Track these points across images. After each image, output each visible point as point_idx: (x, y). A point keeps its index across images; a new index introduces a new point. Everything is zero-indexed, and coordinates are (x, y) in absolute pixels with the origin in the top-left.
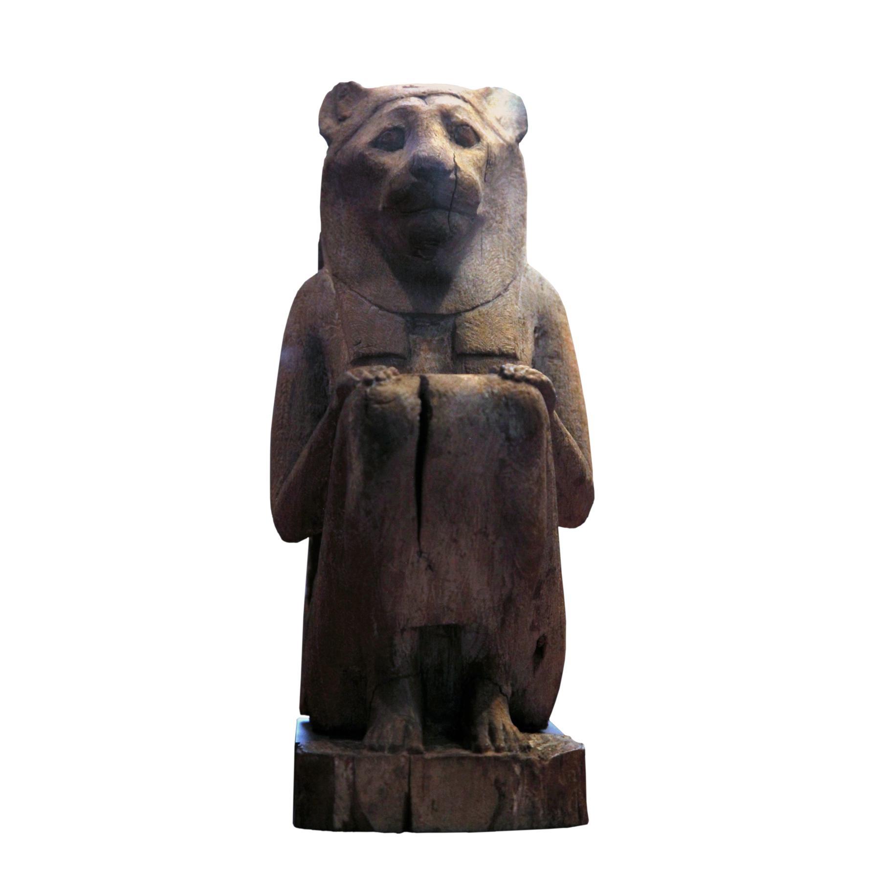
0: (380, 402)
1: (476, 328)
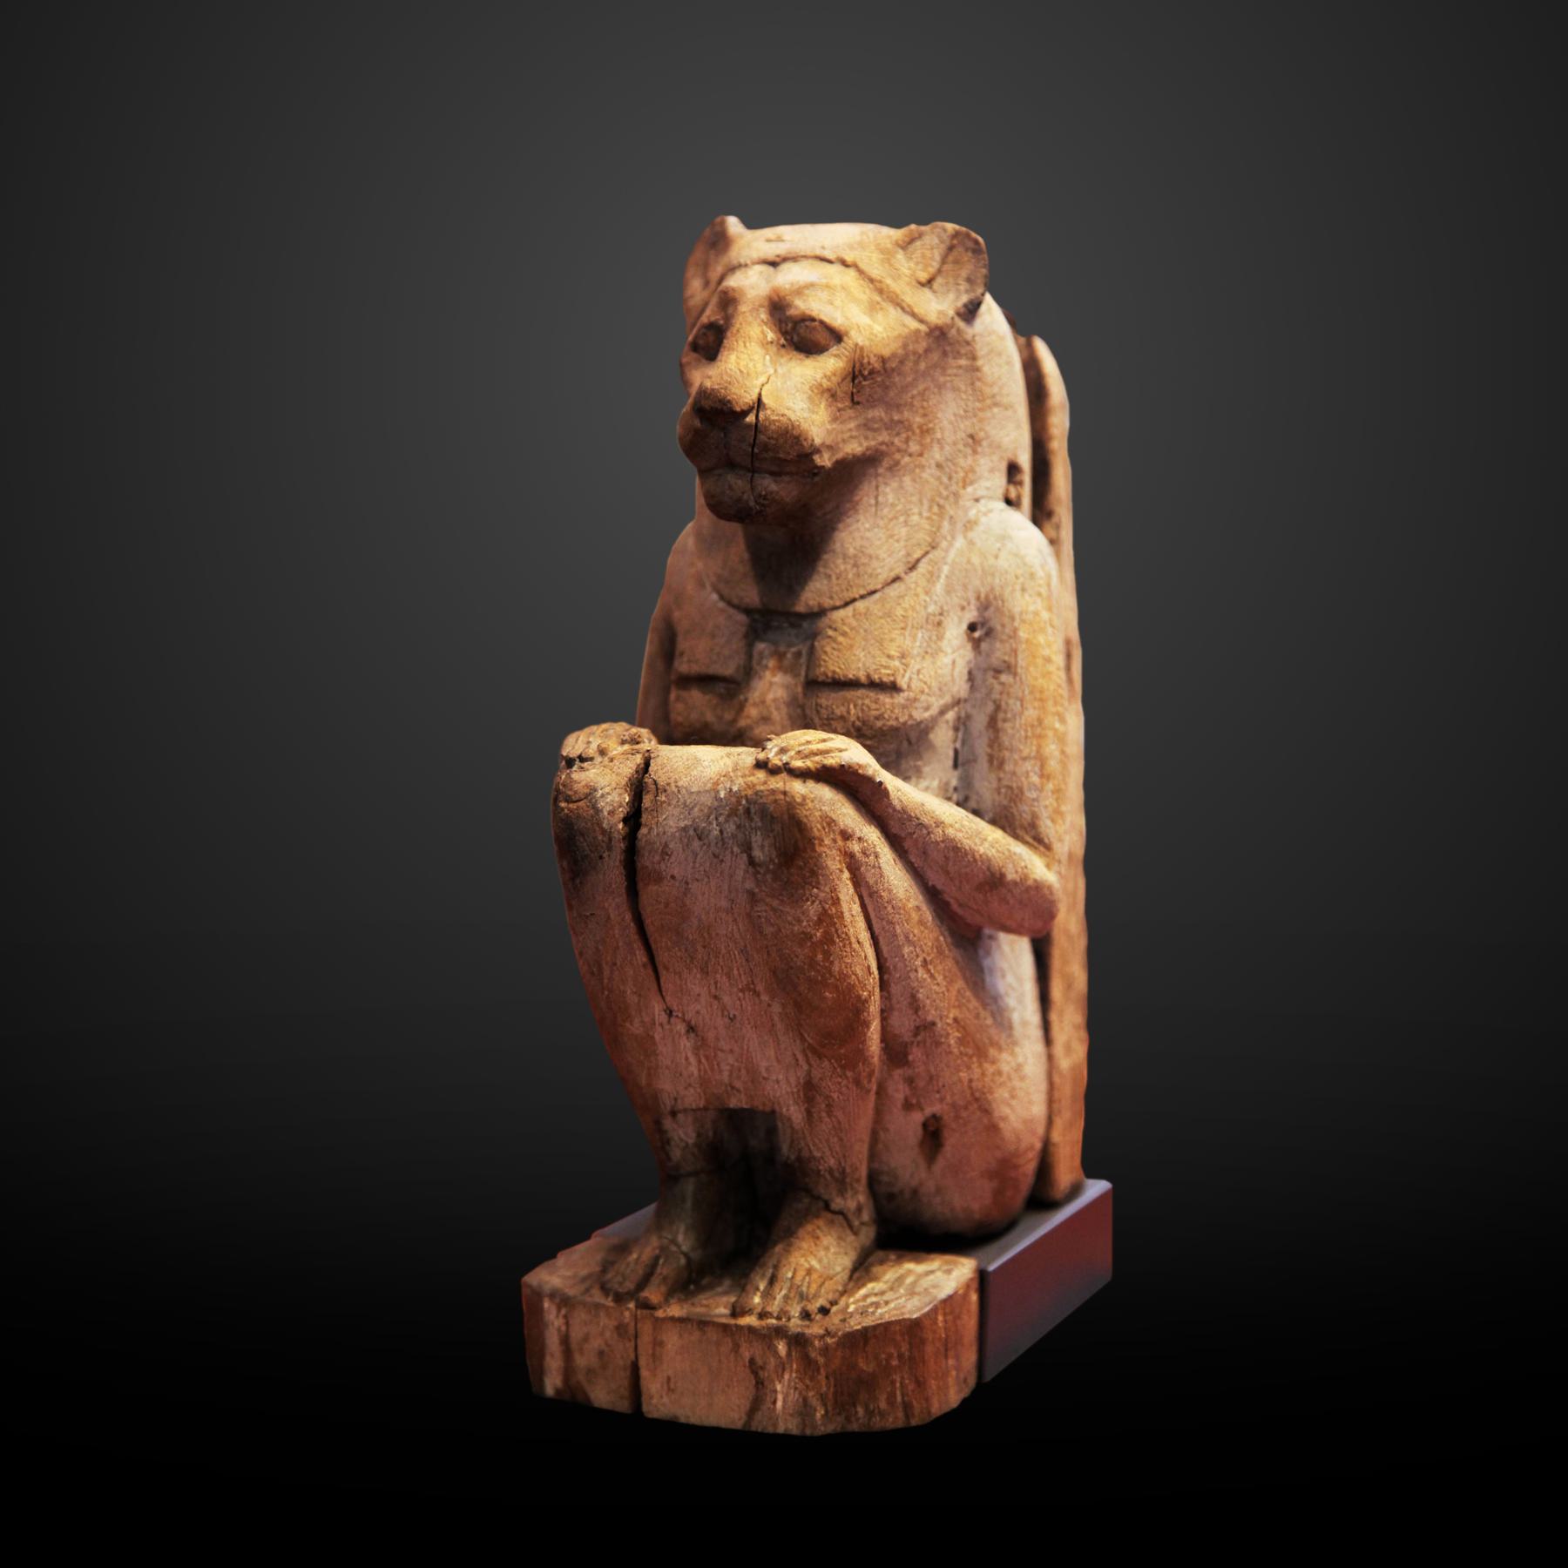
0: (568, 800)
1: (841, 639)
